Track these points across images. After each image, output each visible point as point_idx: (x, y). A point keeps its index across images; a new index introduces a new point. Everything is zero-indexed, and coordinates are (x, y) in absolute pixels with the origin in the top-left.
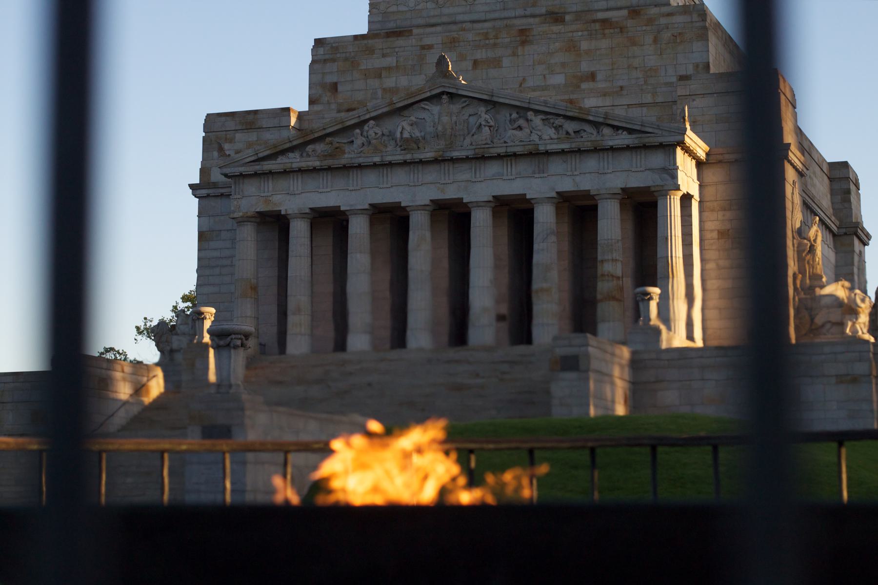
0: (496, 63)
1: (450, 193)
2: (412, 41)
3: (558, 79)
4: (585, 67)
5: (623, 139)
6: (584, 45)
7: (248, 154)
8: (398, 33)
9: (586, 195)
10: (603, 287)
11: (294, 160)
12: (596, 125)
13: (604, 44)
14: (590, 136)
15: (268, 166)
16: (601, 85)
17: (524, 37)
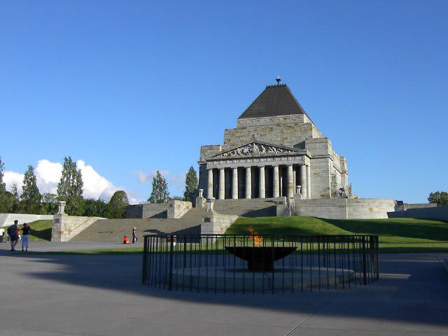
0: (266, 135)
1: (255, 165)
2: (246, 130)
3: (279, 139)
4: (285, 136)
5: (293, 153)
6: (285, 131)
7: (211, 156)
8: (244, 128)
9: (285, 165)
10: (290, 185)
11: (222, 157)
12: (288, 150)
13: (289, 131)
14: (286, 152)
15: (216, 158)
16: (289, 140)
17: (271, 129)
